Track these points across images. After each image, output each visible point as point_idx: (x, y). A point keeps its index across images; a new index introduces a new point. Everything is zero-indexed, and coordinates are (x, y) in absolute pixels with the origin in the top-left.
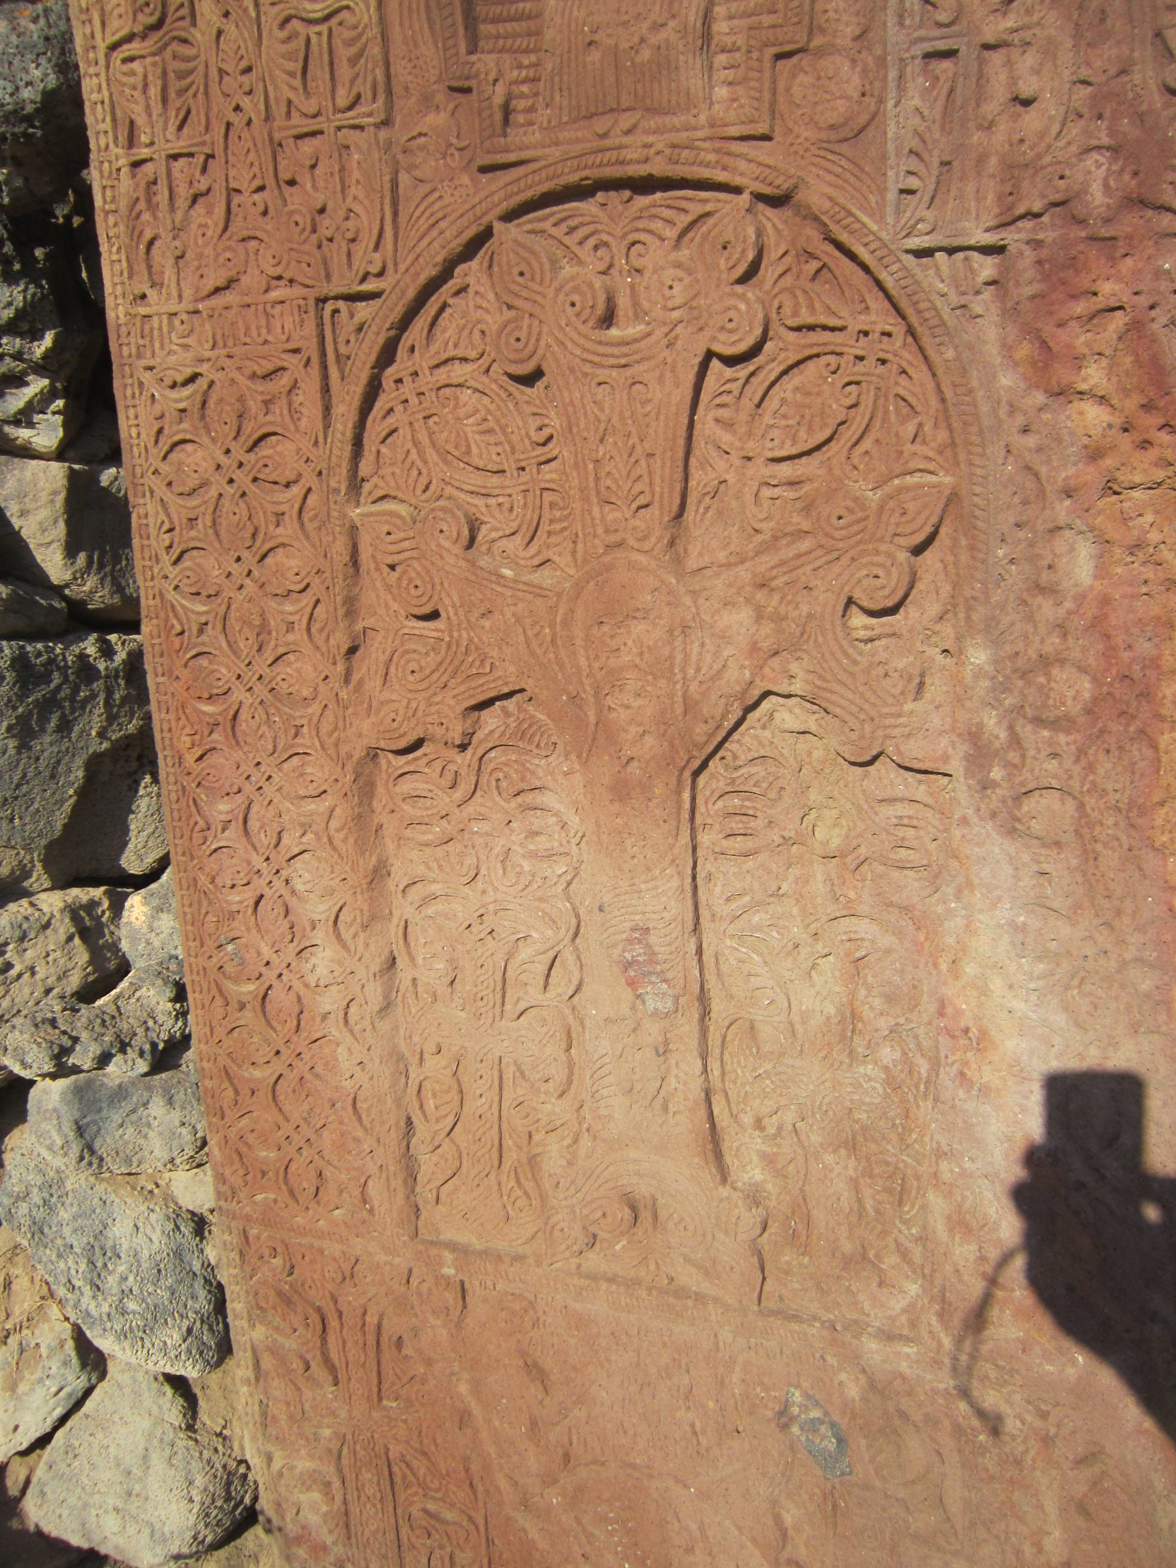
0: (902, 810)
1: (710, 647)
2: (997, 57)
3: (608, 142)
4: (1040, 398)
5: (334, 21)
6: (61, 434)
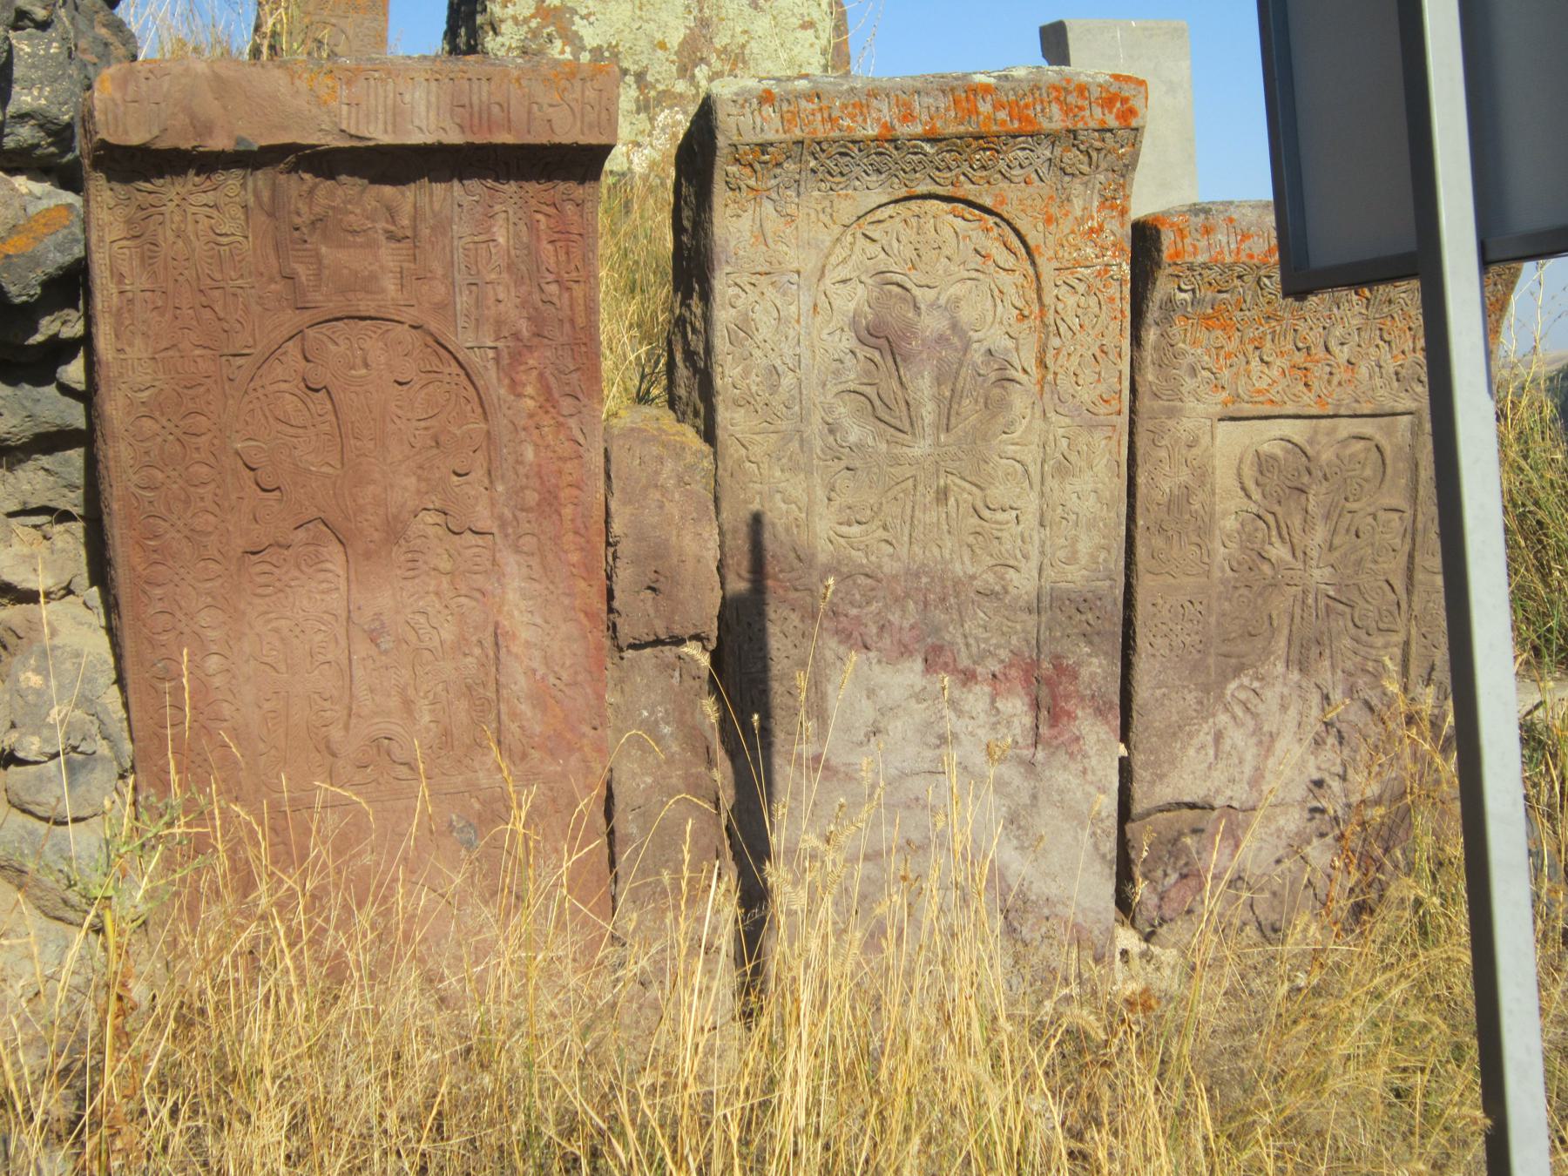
0: (476, 550)
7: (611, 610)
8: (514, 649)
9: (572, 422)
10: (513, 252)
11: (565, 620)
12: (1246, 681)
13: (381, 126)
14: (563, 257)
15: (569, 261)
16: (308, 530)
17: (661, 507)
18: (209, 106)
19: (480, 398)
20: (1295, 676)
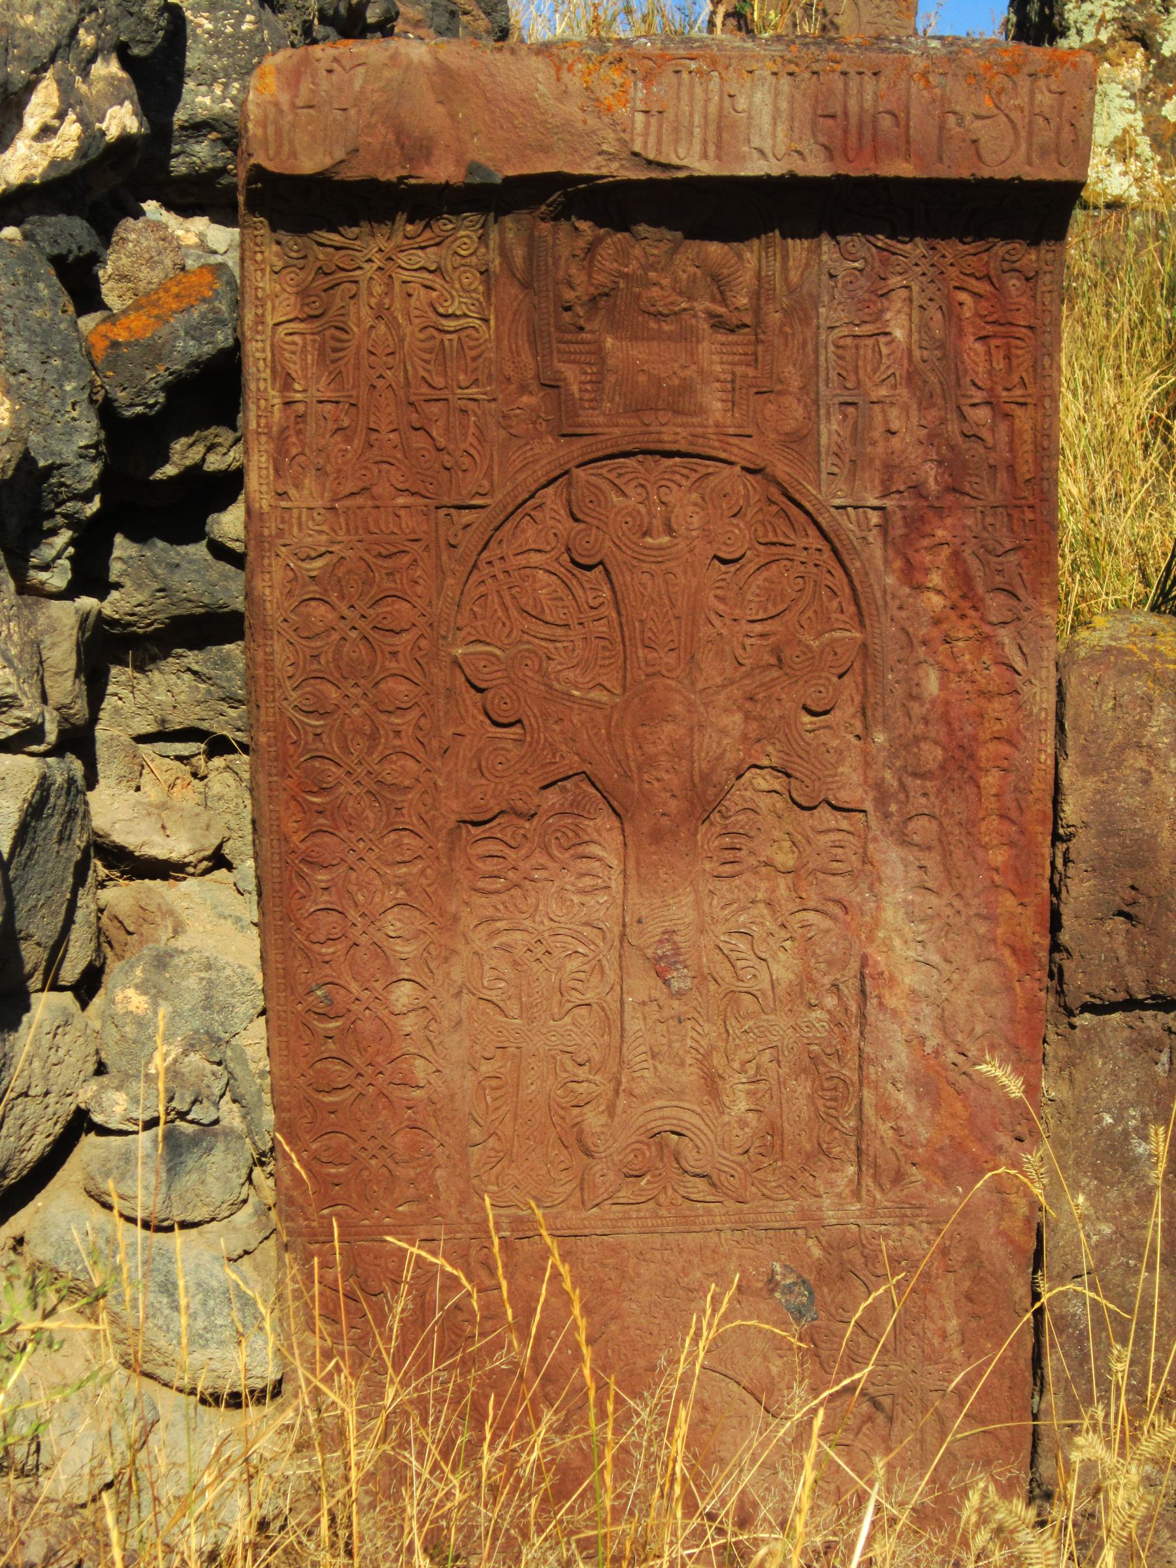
1: (715, 738)
2: (877, 408)
3: (652, 429)
4: (907, 590)
5: (464, 334)
6: (69, 576)
7: (1056, 947)
8: (892, 1002)
9: (1005, 635)
10: (917, 353)
11: (978, 961)
13: (697, 147)
14: (1000, 364)
15: (1010, 369)
16: (564, 790)
17: (1146, 781)
18: (429, 114)
19: (853, 589)
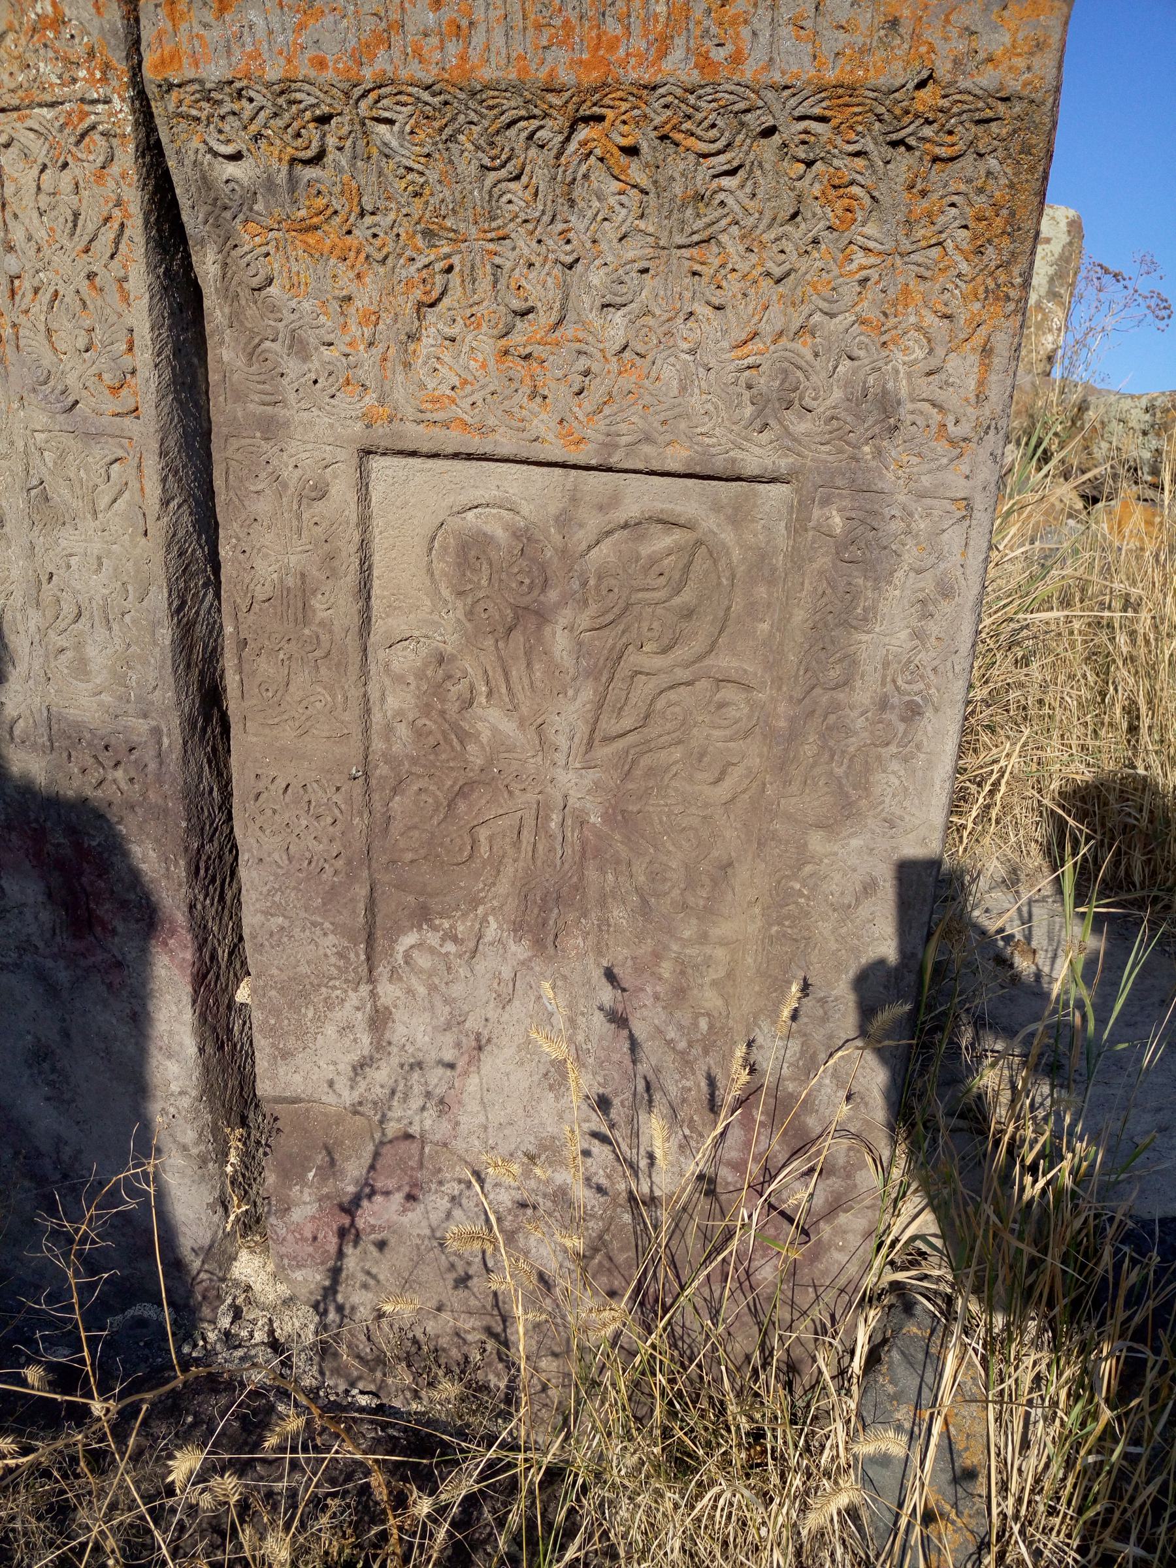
12: (433, 939)
20: (519, 950)
